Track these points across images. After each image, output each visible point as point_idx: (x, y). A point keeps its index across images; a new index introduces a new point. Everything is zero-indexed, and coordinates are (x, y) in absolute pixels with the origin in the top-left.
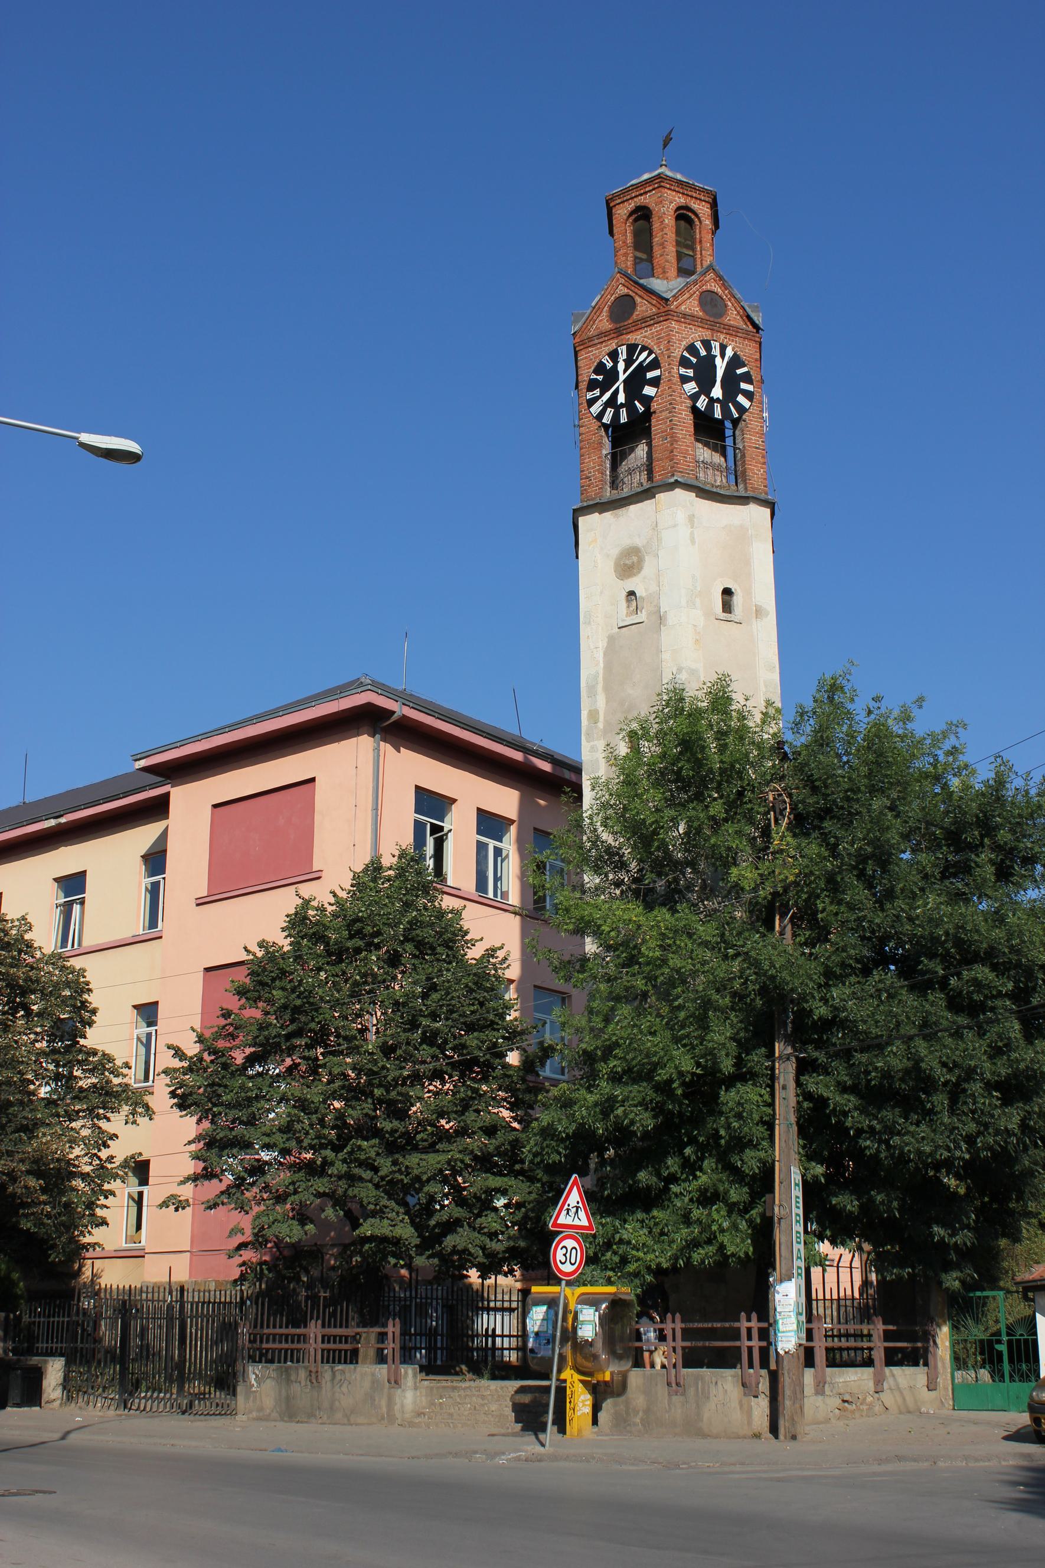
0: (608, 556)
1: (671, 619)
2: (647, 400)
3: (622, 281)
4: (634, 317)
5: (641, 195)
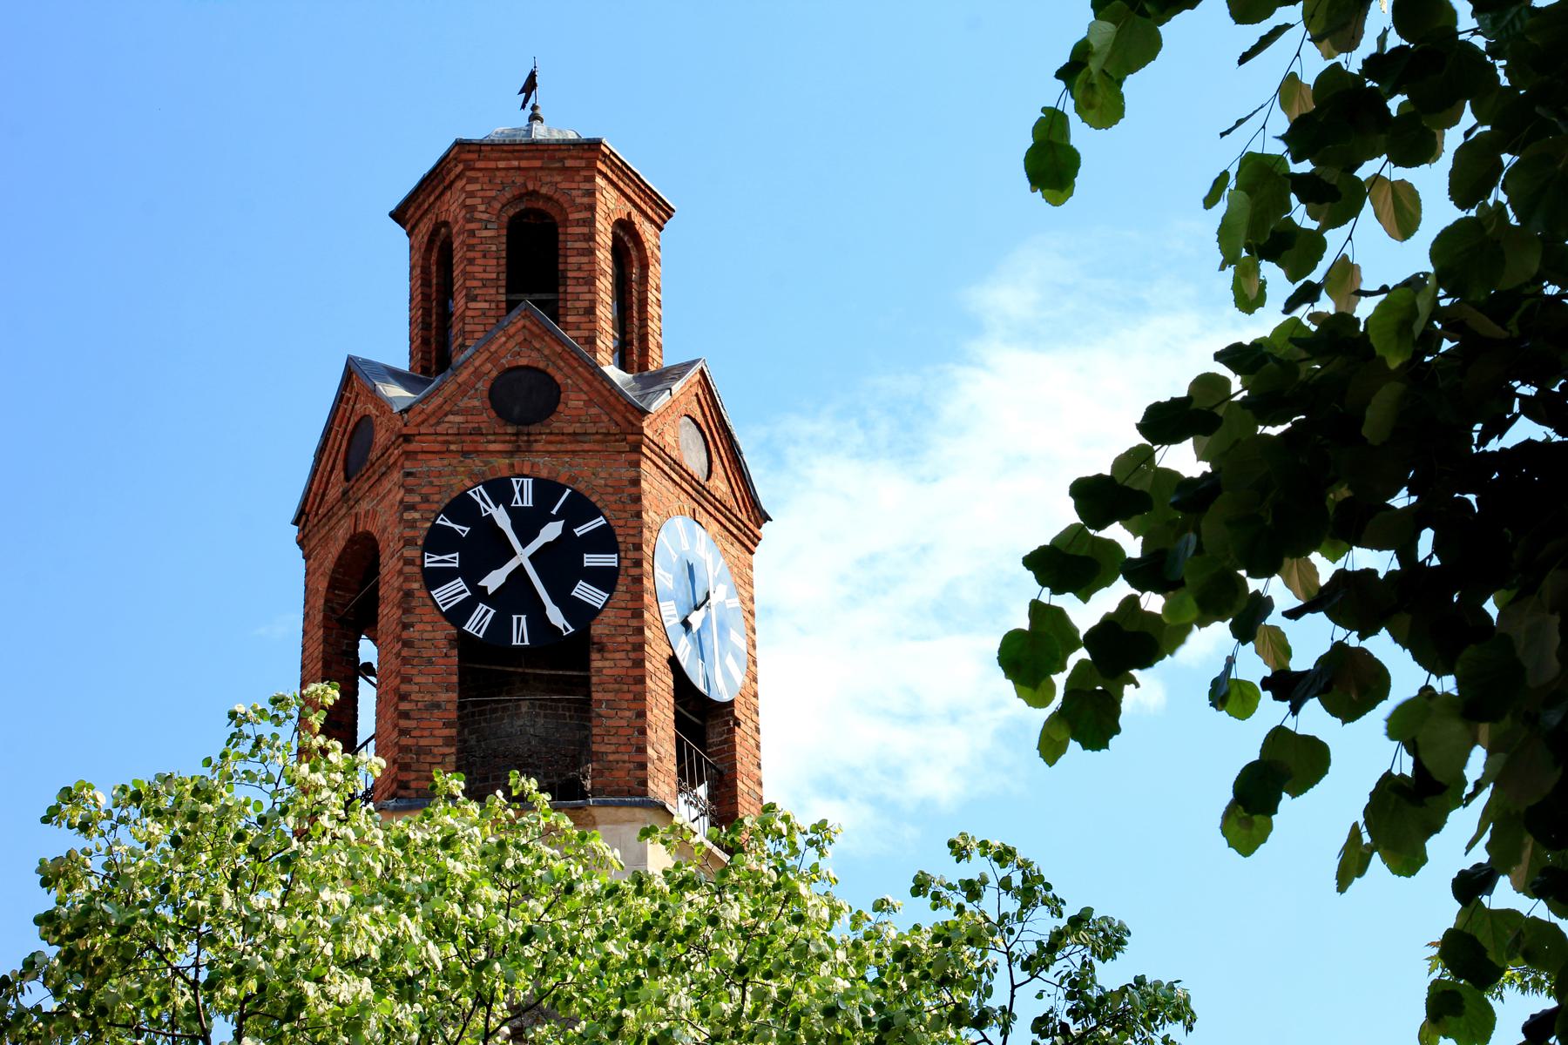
2: (579, 613)
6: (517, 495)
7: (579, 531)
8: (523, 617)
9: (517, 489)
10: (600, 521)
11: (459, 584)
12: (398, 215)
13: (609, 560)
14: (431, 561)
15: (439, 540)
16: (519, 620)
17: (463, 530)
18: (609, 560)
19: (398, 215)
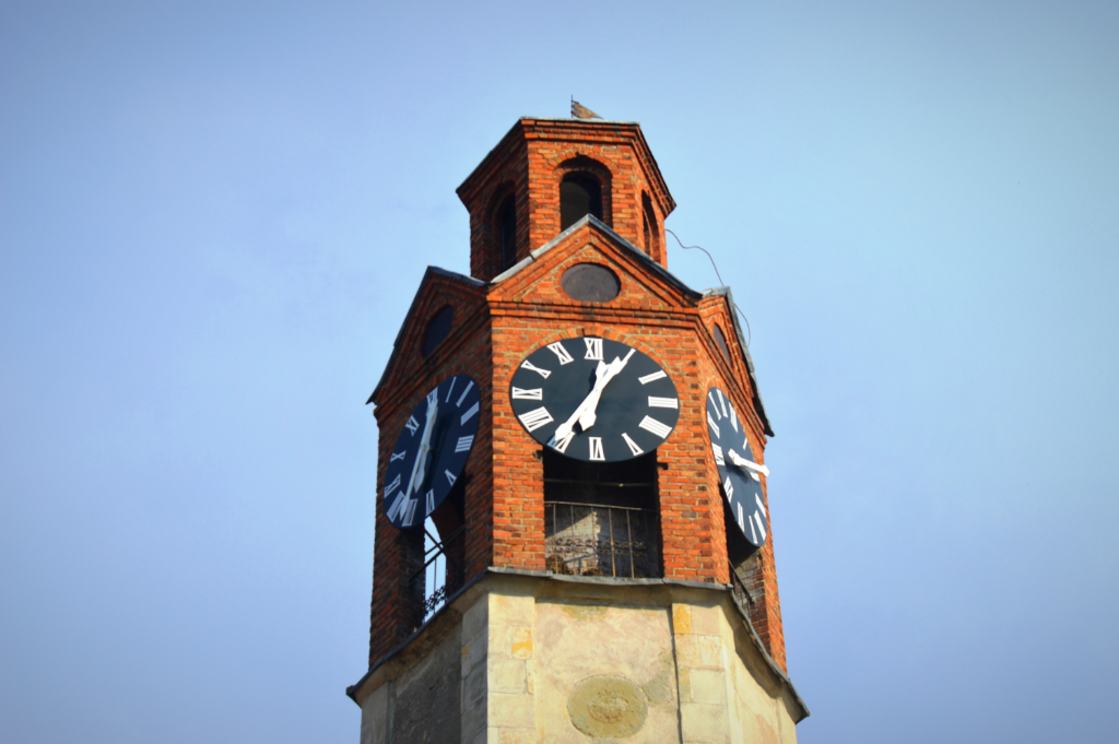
0: (556, 682)
3: (595, 241)
4: (617, 303)
5: (590, 142)
6: (589, 351)
7: (644, 380)
8: (599, 440)
9: (589, 346)
10: (660, 375)
11: (542, 412)
12: (466, 192)
13: (672, 403)
14: (518, 393)
15: (523, 379)
16: (595, 442)
17: (545, 373)
18: (672, 403)
19: (466, 192)
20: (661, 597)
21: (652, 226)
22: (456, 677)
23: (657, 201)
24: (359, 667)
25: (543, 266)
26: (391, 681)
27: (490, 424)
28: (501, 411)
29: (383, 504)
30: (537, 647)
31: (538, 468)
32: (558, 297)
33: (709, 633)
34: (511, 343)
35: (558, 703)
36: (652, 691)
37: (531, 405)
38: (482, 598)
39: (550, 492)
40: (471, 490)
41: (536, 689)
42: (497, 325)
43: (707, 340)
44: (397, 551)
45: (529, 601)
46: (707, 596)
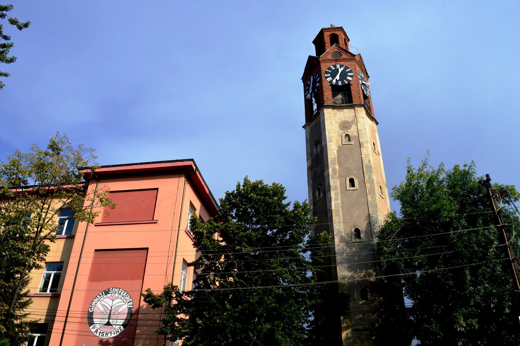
1: (365, 145)
12: (314, 42)
13: (352, 74)
14: (326, 75)
15: (327, 73)
18: (352, 74)
19: (314, 42)
20: (353, 107)
21: (346, 44)
22: (320, 123)
23: (347, 40)
24: (304, 123)
25: (328, 53)
26: (309, 125)
27: (322, 81)
28: (323, 78)
29: (305, 96)
30: (333, 117)
31: (330, 87)
32: (331, 58)
33: (361, 112)
34: (324, 67)
35: (337, 126)
36: (352, 122)
37: (329, 77)
38: (323, 110)
39: (333, 91)
40: (320, 92)
41: (333, 123)
42: (321, 64)
43: (357, 63)
44: (308, 104)
45: (331, 109)
46: (361, 106)
